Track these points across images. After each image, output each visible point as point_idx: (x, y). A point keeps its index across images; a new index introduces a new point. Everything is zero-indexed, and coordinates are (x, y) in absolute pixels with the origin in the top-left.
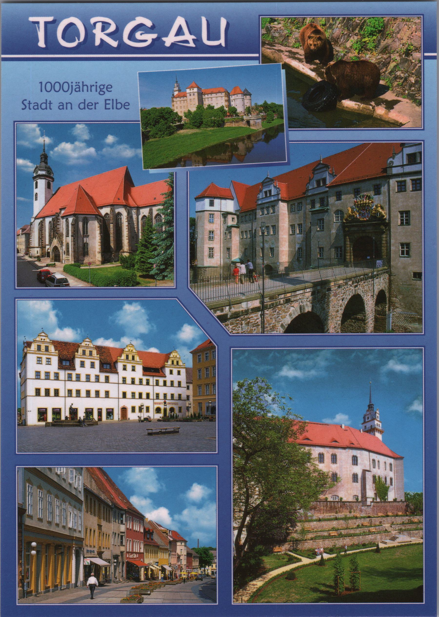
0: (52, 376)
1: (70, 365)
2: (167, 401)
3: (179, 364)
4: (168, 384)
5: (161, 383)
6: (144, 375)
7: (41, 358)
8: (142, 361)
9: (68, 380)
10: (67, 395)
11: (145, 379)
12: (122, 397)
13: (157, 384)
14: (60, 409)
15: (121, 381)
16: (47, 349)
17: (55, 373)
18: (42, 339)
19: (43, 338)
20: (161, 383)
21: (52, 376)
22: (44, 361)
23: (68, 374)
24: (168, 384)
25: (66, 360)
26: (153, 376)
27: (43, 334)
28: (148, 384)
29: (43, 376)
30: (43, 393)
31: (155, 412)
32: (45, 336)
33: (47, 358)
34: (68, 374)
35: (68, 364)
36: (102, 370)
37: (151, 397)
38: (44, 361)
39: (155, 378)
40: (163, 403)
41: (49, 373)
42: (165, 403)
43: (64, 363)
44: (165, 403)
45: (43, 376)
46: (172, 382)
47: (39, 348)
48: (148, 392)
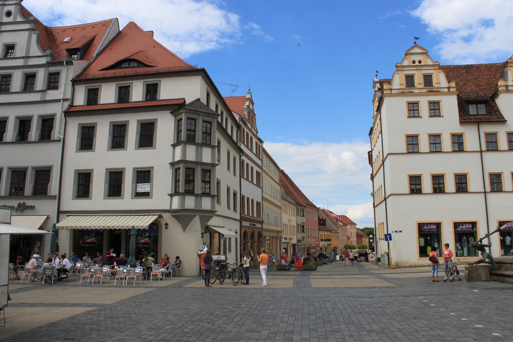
0: (447, 144)
1: (489, 113)
7: (417, 103)
10: (488, 189)
14: (474, 224)
16: (428, 80)
17: (453, 135)
18: (414, 62)
19: (417, 58)
21: (447, 144)
22: (424, 109)
23: (487, 134)
25: (476, 102)
27: (417, 50)
29: (424, 145)
30: (427, 185)
32: (422, 53)
33: (430, 103)
34: (487, 134)
35: (482, 109)
38: (424, 109)
41: (438, 136)
43: (472, 110)
45: (424, 145)
47: (410, 80)
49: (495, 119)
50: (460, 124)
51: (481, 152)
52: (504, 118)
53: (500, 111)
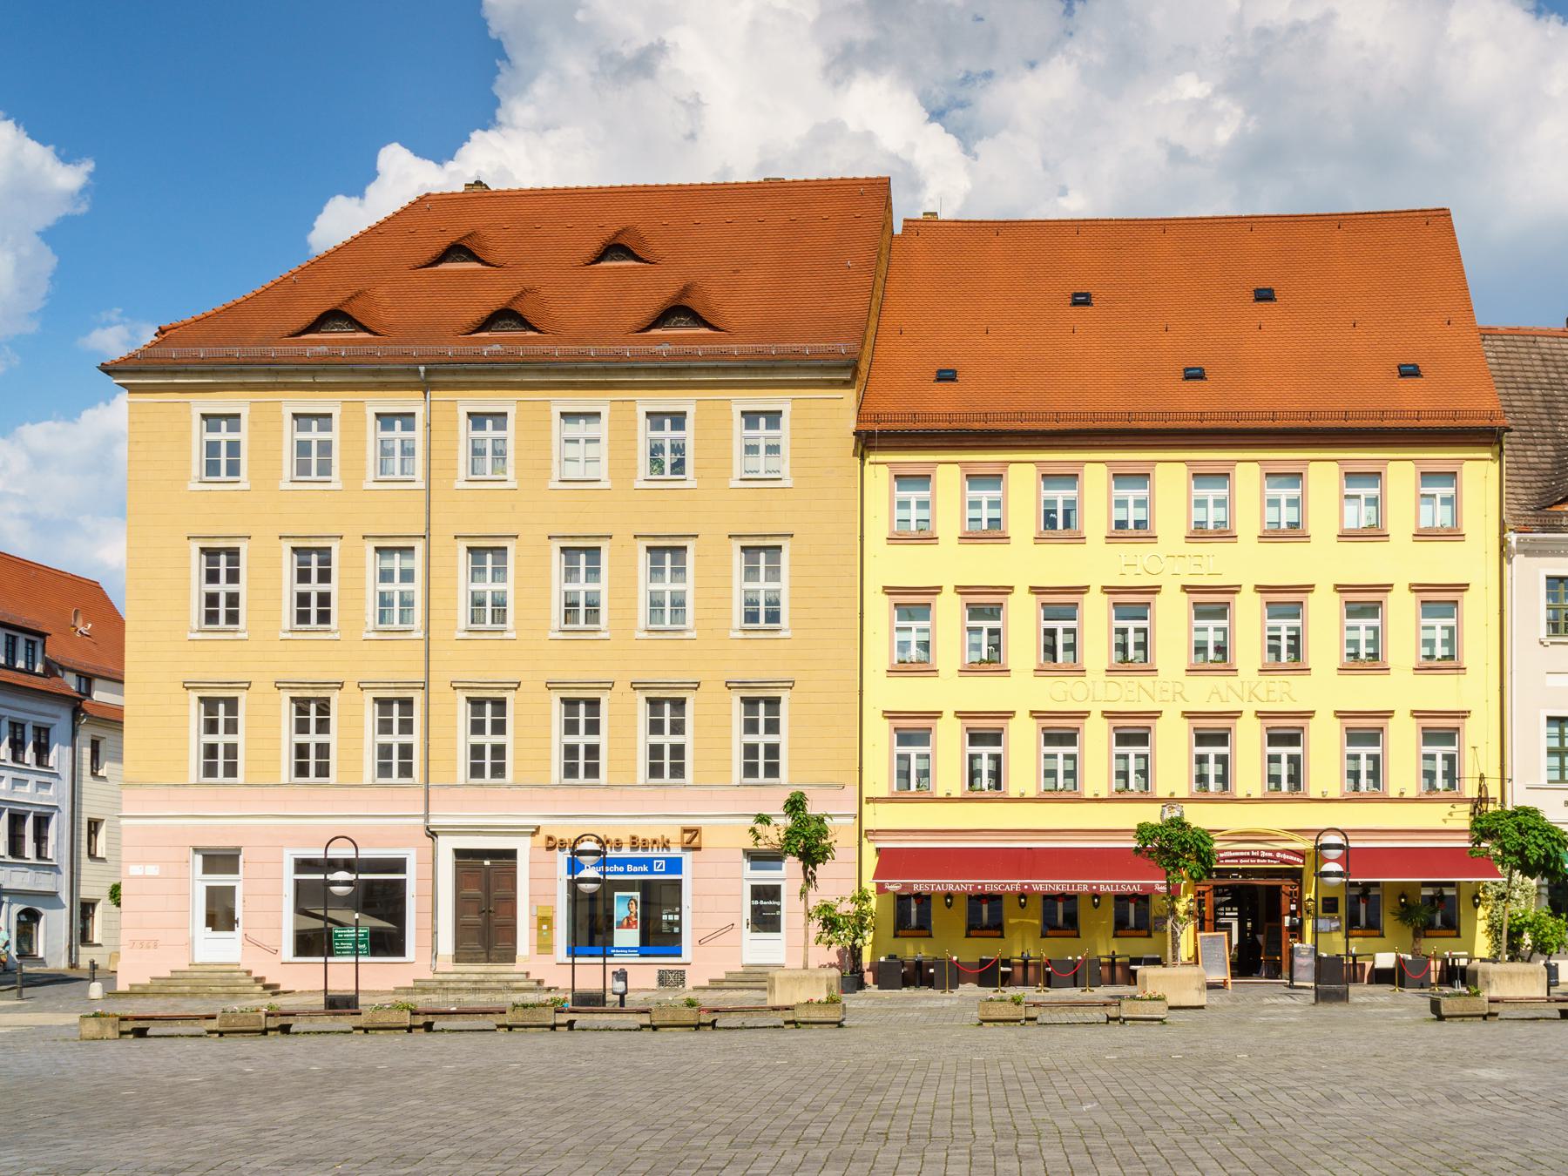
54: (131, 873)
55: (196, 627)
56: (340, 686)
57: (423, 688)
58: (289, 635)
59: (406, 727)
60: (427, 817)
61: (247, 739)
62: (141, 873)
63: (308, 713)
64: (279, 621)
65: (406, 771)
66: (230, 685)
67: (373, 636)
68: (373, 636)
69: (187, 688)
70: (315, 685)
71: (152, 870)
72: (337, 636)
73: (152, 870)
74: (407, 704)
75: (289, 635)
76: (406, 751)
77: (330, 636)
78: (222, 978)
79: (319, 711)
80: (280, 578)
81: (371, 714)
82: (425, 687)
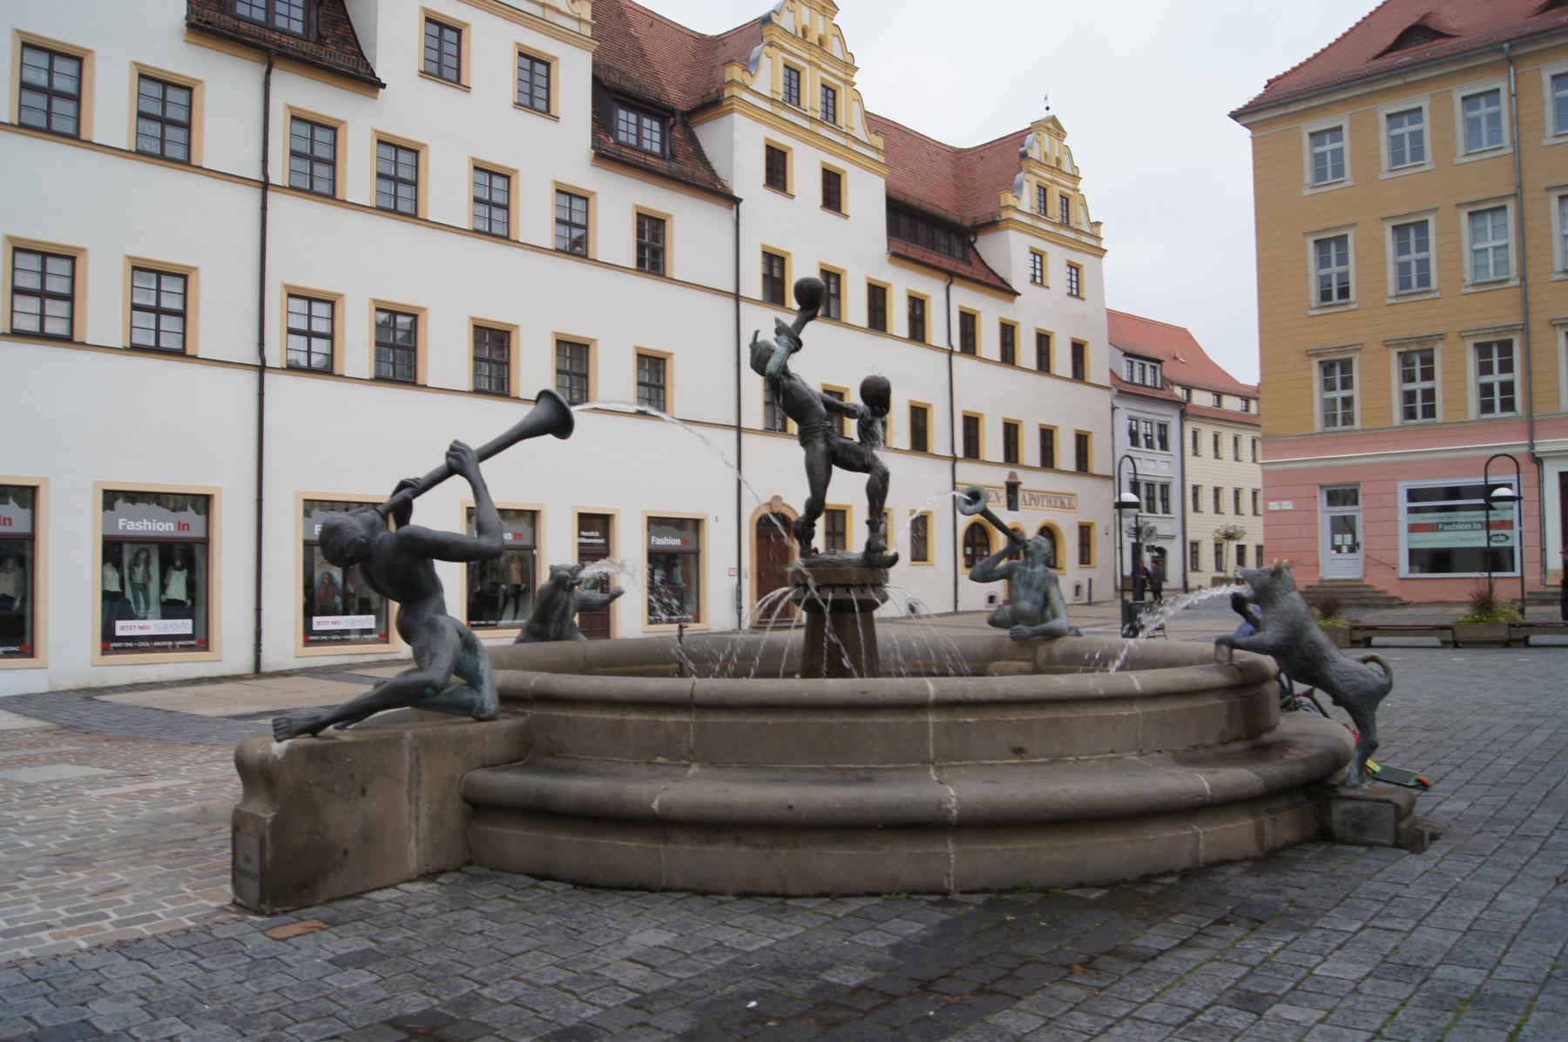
2: (1031, 481)
3: (1072, 224)
4: (1026, 352)
5: (989, 341)
6: (896, 256)
8: (879, 142)
9: (293, 189)
11: (902, 283)
12: (760, 425)
13: (969, 345)
15: (753, 285)
20: (989, 341)
24: (1026, 352)
26: (951, 276)
28: (917, 331)
31: (961, 561)
36: (608, 154)
37: (939, 438)
39: (964, 297)
40: (1003, 493)
42: (1012, 488)
44: (1012, 488)
46: (1043, 340)
48: (921, 399)
49: (339, 65)
50: (188, 31)
51: (265, 186)
52: (373, 74)
53: (359, 47)
54: (1271, 508)
55: (1314, 304)
56: (1441, 337)
57: (1522, 330)
58: (1393, 301)
59: (1507, 367)
60: (1532, 446)
61: (1361, 391)
62: (1277, 508)
63: (1413, 364)
64: (1385, 289)
65: (1508, 405)
66: (1345, 349)
67: (1471, 290)
68: (1471, 290)
69: (1310, 355)
70: (1420, 340)
71: (1287, 505)
72: (1438, 295)
73: (1287, 505)
74: (1506, 347)
75: (1393, 301)
76: (1507, 388)
77: (1432, 296)
78: (1350, 592)
79: (1423, 362)
80: (1384, 254)
81: (1471, 361)
82: (1524, 329)
